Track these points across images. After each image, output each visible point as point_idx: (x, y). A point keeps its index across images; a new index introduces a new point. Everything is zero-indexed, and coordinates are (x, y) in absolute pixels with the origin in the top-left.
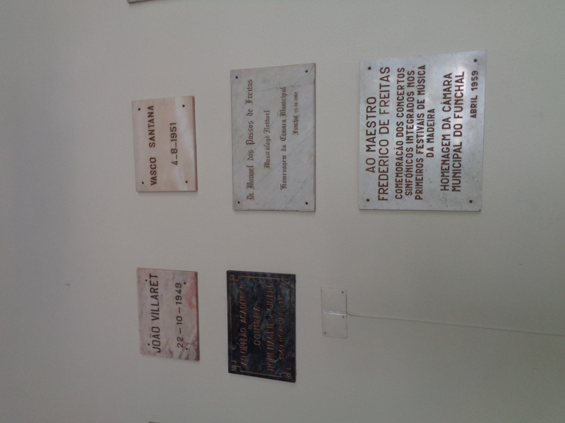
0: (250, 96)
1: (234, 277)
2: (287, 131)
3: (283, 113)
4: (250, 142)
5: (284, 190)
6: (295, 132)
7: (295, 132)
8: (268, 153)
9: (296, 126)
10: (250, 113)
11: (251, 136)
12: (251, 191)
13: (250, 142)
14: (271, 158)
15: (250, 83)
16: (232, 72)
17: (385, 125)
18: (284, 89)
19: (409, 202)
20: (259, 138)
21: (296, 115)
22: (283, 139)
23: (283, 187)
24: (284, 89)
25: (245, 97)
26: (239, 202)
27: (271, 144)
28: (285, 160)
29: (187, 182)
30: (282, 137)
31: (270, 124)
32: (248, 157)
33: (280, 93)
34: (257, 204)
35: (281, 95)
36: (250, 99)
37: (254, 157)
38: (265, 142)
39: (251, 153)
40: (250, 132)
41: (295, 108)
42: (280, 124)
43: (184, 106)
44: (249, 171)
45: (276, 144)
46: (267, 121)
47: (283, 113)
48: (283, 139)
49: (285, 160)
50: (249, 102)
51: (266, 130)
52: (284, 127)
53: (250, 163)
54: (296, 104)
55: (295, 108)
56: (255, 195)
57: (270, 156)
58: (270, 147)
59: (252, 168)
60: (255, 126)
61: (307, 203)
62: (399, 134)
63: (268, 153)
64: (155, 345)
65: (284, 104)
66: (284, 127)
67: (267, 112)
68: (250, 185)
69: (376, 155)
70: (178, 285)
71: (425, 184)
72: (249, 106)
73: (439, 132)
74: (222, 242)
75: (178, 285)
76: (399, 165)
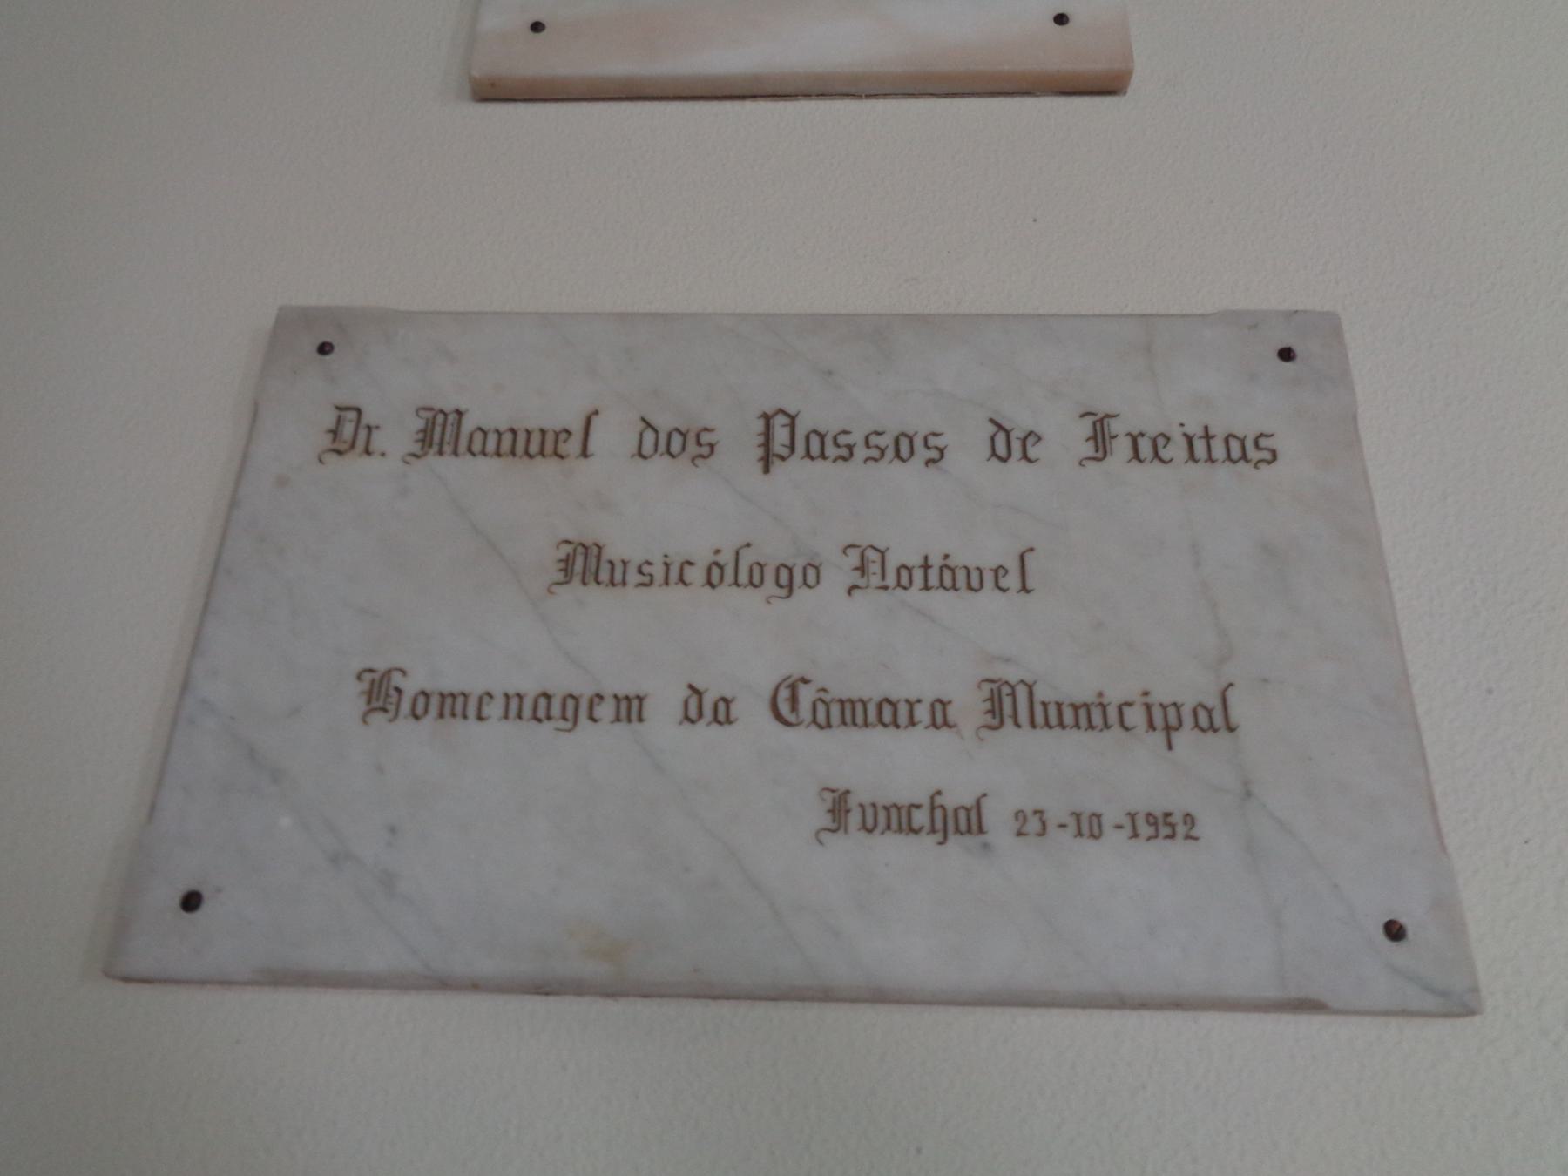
0: (1149, 448)
2: (855, 735)
3: (1006, 704)
4: (779, 440)
5: (351, 696)
6: (839, 806)
7: (839, 806)
8: (676, 573)
9: (895, 819)
10: (1010, 443)
11: (825, 446)
12: (397, 437)
13: (781, 435)
14: (632, 594)
15: (1251, 451)
16: (1330, 327)
18: (1216, 719)
20: (810, 506)
21: (997, 817)
22: (787, 702)
23: (380, 693)
24: (1216, 719)
25: (1138, 410)
26: (324, 349)
27: (748, 600)
28: (605, 711)
29: (537, 27)
30: (806, 695)
31: (915, 595)
32: (664, 422)
33: (1186, 683)
34: (282, 482)
35: (1162, 695)
36: (1122, 447)
37: (660, 463)
38: (773, 549)
39: (689, 444)
40: (857, 438)
41: (1057, 812)
42: (915, 679)
43: (1061, 19)
44: (553, 423)
45: (746, 644)
46: (946, 576)
47: (1006, 704)
48: (787, 702)
49: (605, 711)
50: (1101, 440)
51: (867, 564)
52: (890, 713)
53: (613, 436)
54: (1088, 826)
55: (1057, 812)
56: (355, 464)
57: (657, 593)
58: (727, 593)
59: (573, 446)
60: (908, 476)
61: (191, 902)
63: (676, 573)
65: (1086, 715)
66: (890, 713)
67: (1015, 575)
68: (440, 432)
72: (1065, 436)
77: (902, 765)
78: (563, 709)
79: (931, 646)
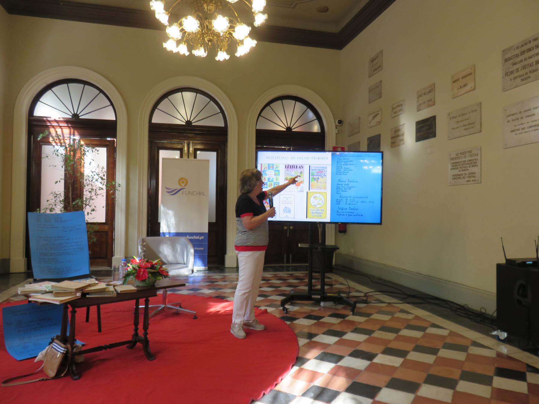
1: (434, 118)
3: (469, 124)
4: (463, 115)
15: (476, 111)
17: (466, 157)
19: (450, 167)
39: (460, 116)
46: (467, 119)
47: (469, 124)
62: (464, 161)
73: (464, 172)
76: (457, 163)
77: (466, 127)
79: (466, 122)
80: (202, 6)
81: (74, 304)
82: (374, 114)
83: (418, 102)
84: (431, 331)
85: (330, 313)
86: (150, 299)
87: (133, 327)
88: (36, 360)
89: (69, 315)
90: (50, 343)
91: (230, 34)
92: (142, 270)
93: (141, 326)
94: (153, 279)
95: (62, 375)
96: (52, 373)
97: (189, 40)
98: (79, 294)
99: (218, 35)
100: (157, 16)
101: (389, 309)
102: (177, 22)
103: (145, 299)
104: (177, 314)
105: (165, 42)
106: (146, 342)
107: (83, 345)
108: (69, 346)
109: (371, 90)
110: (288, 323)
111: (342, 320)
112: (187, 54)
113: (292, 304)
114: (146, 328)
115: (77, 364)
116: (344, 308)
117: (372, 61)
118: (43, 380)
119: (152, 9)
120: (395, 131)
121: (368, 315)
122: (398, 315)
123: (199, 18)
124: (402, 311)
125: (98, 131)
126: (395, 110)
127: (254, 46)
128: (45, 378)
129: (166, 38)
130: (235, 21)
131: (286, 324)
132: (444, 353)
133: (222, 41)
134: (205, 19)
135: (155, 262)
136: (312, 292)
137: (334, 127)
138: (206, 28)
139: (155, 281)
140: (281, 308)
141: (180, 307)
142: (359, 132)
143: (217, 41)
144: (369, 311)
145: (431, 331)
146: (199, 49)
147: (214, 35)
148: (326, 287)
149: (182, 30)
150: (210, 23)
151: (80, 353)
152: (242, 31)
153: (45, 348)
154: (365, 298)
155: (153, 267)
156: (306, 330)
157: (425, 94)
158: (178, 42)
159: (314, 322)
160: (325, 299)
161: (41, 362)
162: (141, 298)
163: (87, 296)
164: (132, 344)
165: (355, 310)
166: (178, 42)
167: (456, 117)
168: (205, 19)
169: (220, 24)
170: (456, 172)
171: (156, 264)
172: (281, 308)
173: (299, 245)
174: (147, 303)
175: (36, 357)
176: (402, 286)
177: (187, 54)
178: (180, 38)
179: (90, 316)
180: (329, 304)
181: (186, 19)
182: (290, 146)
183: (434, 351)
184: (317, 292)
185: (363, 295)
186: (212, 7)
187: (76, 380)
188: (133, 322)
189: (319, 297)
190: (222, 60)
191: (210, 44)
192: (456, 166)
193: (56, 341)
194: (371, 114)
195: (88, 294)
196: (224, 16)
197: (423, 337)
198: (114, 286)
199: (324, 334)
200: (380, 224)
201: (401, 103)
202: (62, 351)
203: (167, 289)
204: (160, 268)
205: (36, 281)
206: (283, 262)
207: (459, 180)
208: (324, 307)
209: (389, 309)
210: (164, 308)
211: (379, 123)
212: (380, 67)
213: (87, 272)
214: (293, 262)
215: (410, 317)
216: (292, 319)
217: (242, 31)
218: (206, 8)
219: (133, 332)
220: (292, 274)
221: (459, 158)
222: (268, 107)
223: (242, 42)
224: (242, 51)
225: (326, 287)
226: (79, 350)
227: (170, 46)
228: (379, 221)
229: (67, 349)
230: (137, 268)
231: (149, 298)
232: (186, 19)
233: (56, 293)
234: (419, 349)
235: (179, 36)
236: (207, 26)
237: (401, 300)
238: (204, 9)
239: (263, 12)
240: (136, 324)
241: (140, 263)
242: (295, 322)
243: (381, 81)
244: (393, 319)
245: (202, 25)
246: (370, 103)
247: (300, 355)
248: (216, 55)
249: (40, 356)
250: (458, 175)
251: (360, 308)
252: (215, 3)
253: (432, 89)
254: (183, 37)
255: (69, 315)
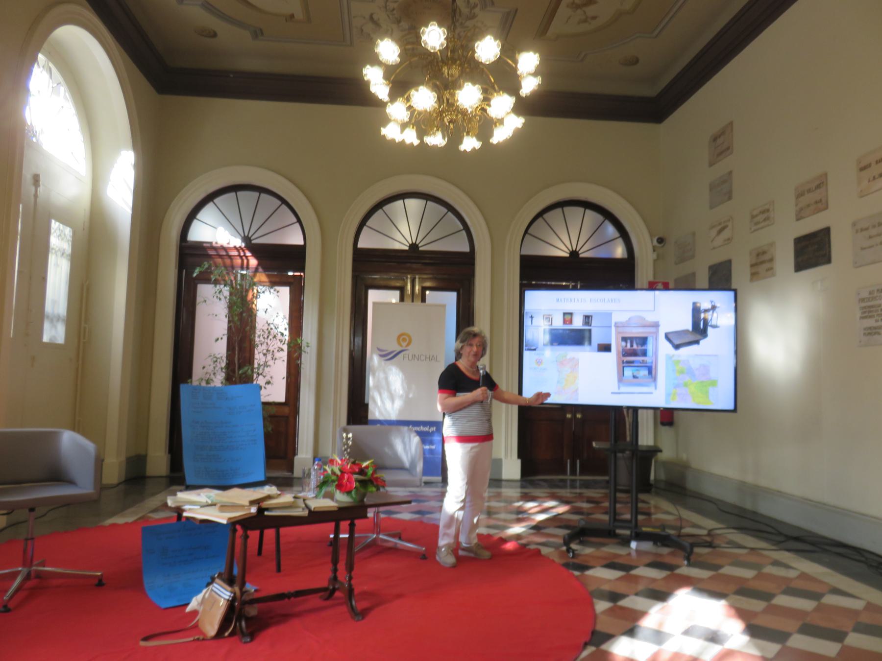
1: (827, 231)
19: (858, 314)
39: (874, 226)
64: (799, 195)
69: (876, 294)
70: (821, 200)
71: (865, 321)
74: (839, 219)
75: (821, 200)
76: (872, 306)
78: (870, 247)
80: (440, 70)
81: (246, 523)
82: (720, 227)
83: (796, 205)
84: (830, 600)
85: (648, 560)
86: (357, 522)
87: (330, 567)
88: (189, 609)
89: (239, 542)
90: (208, 584)
91: (484, 110)
92: (346, 476)
93: (341, 566)
94: (362, 490)
95: (227, 634)
96: (211, 629)
97: (421, 122)
98: (253, 510)
99: (464, 113)
100: (373, 89)
101: (753, 559)
102: (402, 95)
103: (349, 522)
104: (394, 550)
105: (384, 126)
106: (350, 592)
107: (256, 591)
108: (237, 589)
109: (712, 187)
110: (577, 573)
111: (668, 573)
112: (416, 142)
113: (581, 543)
114: (350, 568)
115: (248, 620)
116: (672, 554)
117: (715, 139)
118: (198, 639)
119: (366, 79)
120: (758, 255)
121: (716, 567)
122: (769, 570)
123: (435, 88)
124: (776, 563)
125: (281, 263)
126: (756, 220)
127: (520, 126)
128: (201, 637)
129: (385, 120)
130: (490, 90)
131: (573, 575)
132: (855, 640)
133: (470, 120)
134: (446, 89)
135: (364, 465)
136: (617, 524)
137: (650, 249)
138: (446, 104)
139: (364, 495)
140: (564, 548)
141: (400, 538)
142: (693, 257)
143: (462, 122)
144: (718, 561)
145: (830, 600)
146: (434, 134)
147: (458, 112)
148: (640, 517)
149: (410, 108)
150: (453, 95)
151: (252, 602)
152: (501, 105)
153: (200, 591)
154: (708, 539)
155: (362, 472)
156: (606, 587)
157: (809, 191)
158: (404, 126)
159: (618, 574)
160: (640, 536)
161: (195, 613)
162: (345, 519)
163: (266, 513)
164: (329, 593)
165: (693, 558)
166: (404, 126)
167: (867, 229)
168: (446, 89)
169: (468, 96)
170: (871, 323)
171: (367, 467)
172: (564, 548)
173: (594, 444)
174: (352, 526)
175: (187, 604)
176: (775, 520)
177: (416, 142)
178: (406, 119)
179: (264, 547)
180: (647, 546)
181: (417, 90)
182: (575, 281)
183: (837, 636)
184: (625, 524)
185: (705, 532)
186: (455, 71)
187: (245, 643)
188: (329, 558)
189: (627, 532)
190: (469, 150)
191: (451, 126)
192: (870, 312)
193: (217, 580)
194: (713, 227)
195: (267, 509)
196: (474, 84)
197: (817, 609)
198: (304, 500)
199: (637, 594)
200: (735, 410)
201: (767, 207)
202: (227, 598)
203: (381, 509)
204: (373, 474)
205: (189, 488)
206: (565, 473)
207: (876, 337)
208: (637, 551)
209: (753, 559)
210: (375, 540)
211: (729, 240)
212: (728, 148)
213: (262, 478)
214: (581, 473)
215: (792, 574)
216: (583, 568)
217: (501, 105)
218: (446, 72)
219: (330, 575)
220: (580, 494)
221: (874, 298)
222: (540, 219)
223: (501, 121)
224: (500, 135)
225: (640, 517)
226: (251, 597)
227: (391, 132)
228: (731, 406)
229: (235, 594)
230: (339, 473)
231: (357, 522)
232: (417, 90)
233: (222, 506)
234: (808, 630)
235: (404, 116)
236: (448, 100)
237: (774, 545)
238: (443, 74)
239: (535, 74)
240: (335, 562)
241: (342, 464)
242: (589, 573)
243: (730, 173)
244: (760, 576)
245: (440, 100)
246: (711, 207)
247: (599, 627)
248: (461, 142)
249: (194, 604)
250: (875, 328)
251: (700, 555)
252: (460, 65)
253: (821, 183)
254: (411, 118)
255: (239, 542)
